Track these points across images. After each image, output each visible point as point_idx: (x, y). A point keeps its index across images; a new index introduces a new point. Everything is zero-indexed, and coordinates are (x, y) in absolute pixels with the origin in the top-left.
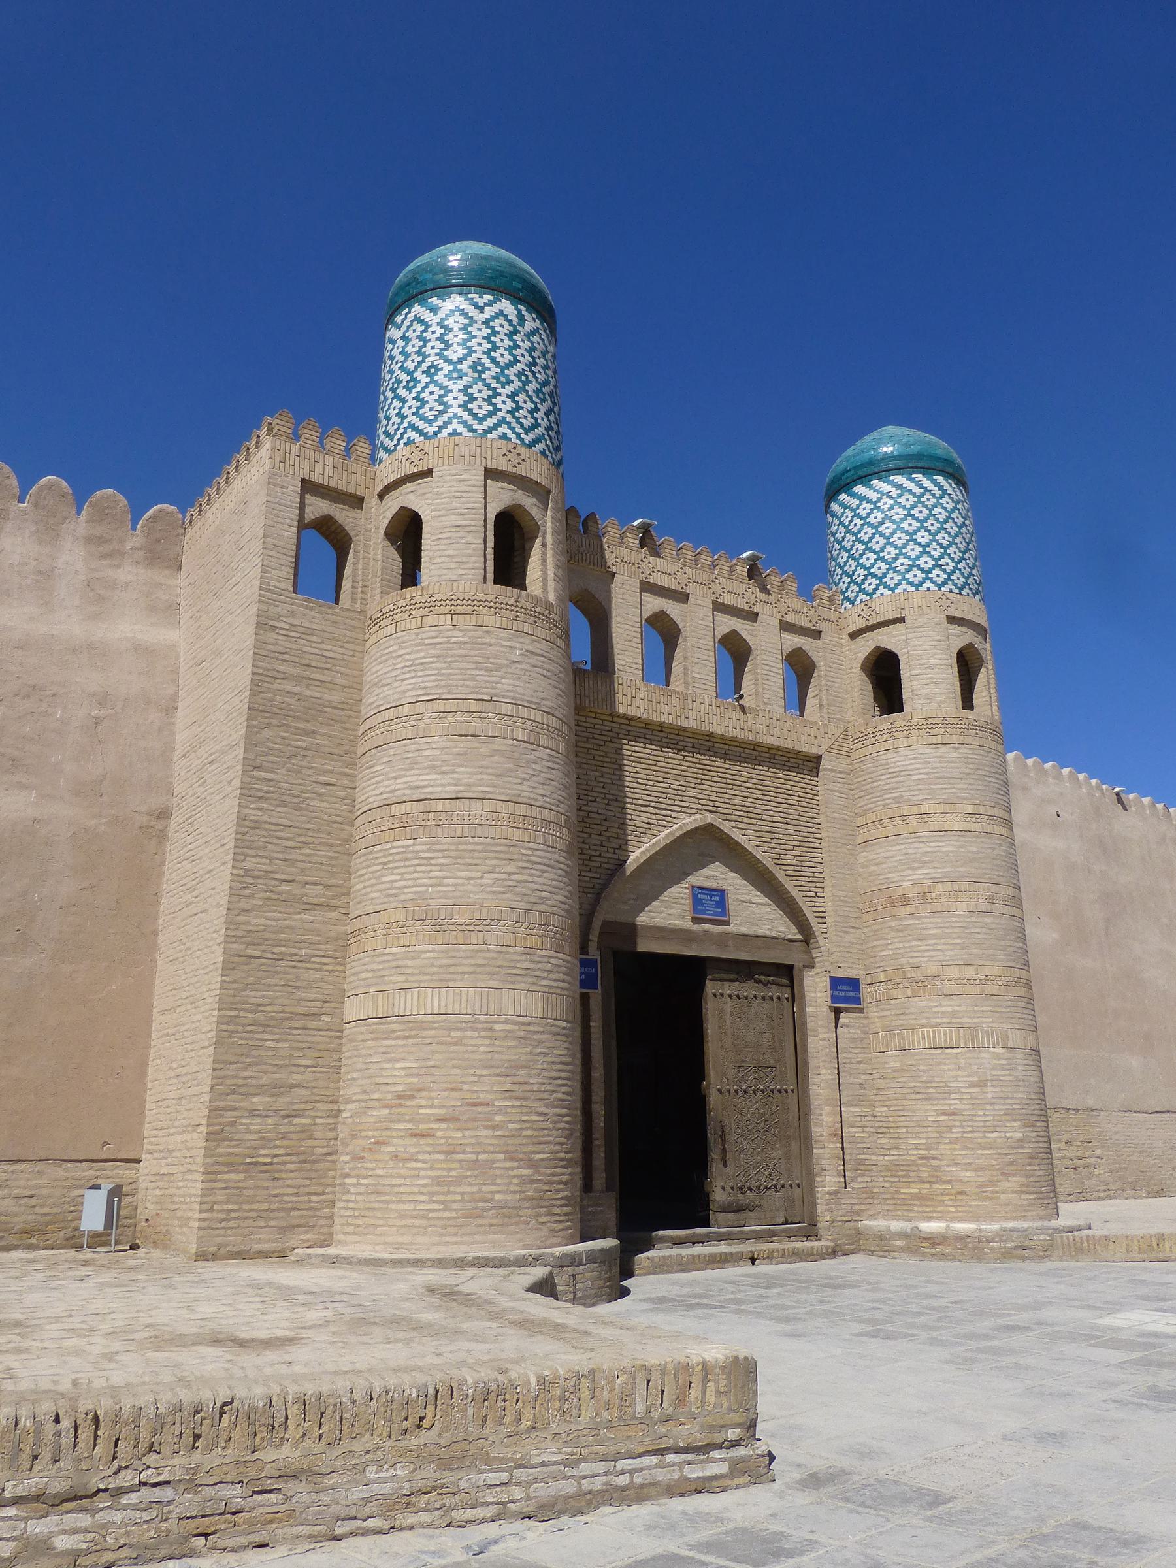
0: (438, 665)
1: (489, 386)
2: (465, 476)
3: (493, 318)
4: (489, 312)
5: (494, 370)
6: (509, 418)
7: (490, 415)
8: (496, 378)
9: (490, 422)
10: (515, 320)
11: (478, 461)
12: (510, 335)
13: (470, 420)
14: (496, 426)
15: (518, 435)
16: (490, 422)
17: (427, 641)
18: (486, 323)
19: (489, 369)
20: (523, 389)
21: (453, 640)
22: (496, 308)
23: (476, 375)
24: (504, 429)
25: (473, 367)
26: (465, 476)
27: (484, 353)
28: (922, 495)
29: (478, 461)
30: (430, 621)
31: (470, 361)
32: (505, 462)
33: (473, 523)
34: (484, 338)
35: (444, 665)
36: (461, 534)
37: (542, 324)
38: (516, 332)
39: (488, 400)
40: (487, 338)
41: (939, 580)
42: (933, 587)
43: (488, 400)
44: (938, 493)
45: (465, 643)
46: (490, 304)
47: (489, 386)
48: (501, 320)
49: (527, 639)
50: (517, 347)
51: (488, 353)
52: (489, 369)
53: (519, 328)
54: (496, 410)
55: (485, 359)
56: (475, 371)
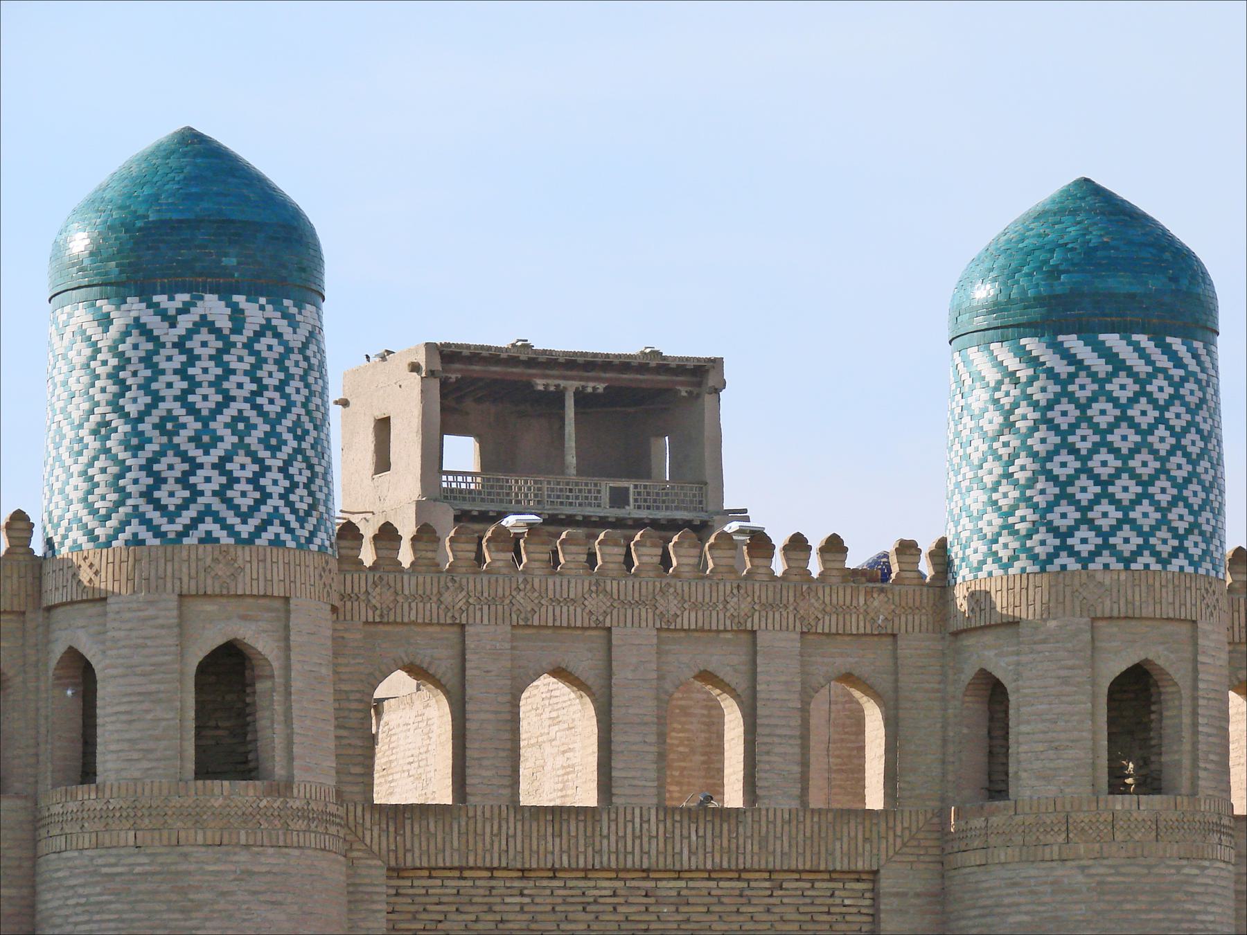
0: (119, 906)
1: (184, 457)
2: (151, 612)
3: (190, 333)
4: (185, 322)
5: (193, 425)
6: (217, 505)
7: (185, 505)
8: (196, 439)
9: (186, 517)
10: (224, 324)
11: (169, 585)
12: (217, 358)
13: (155, 516)
14: (195, 523)
15: (230, 529)
16: (186, 517)
17: (104, 870)
18: (180, 345)
19: (184, 426)
20: (241, 445)
21: (138, 869)
22: (194, 315)
23: (165, 439)
24: (209, 525)
25: (160, 427)
26: (151, 612)
27: (176, 399)
28: (1072, 377)
29: (169, 585)
30: (106, 839)
31: (154, 418)
32: (209, 582)
33: (162, 687)
34: (176, 372)
35: (126, 907)
36: (145, 706)
37: (277, 305)
38: (228, 347)
39: (183, 481)
40: (181, 372)
41: (1085, 550)
42: (1073, 565)
43: (183, 481)
44: (1101, 366)
45: (154, 874)
46: (184, 310)
47: (184, 457)
48: (204, 335)
49: (243, 857)
50: (229, 372)
51: (182, 398)
52: (184, 426)
53: (233, 338)
54: (196, 493)
55: (178, 410)
56: (164, 432)
